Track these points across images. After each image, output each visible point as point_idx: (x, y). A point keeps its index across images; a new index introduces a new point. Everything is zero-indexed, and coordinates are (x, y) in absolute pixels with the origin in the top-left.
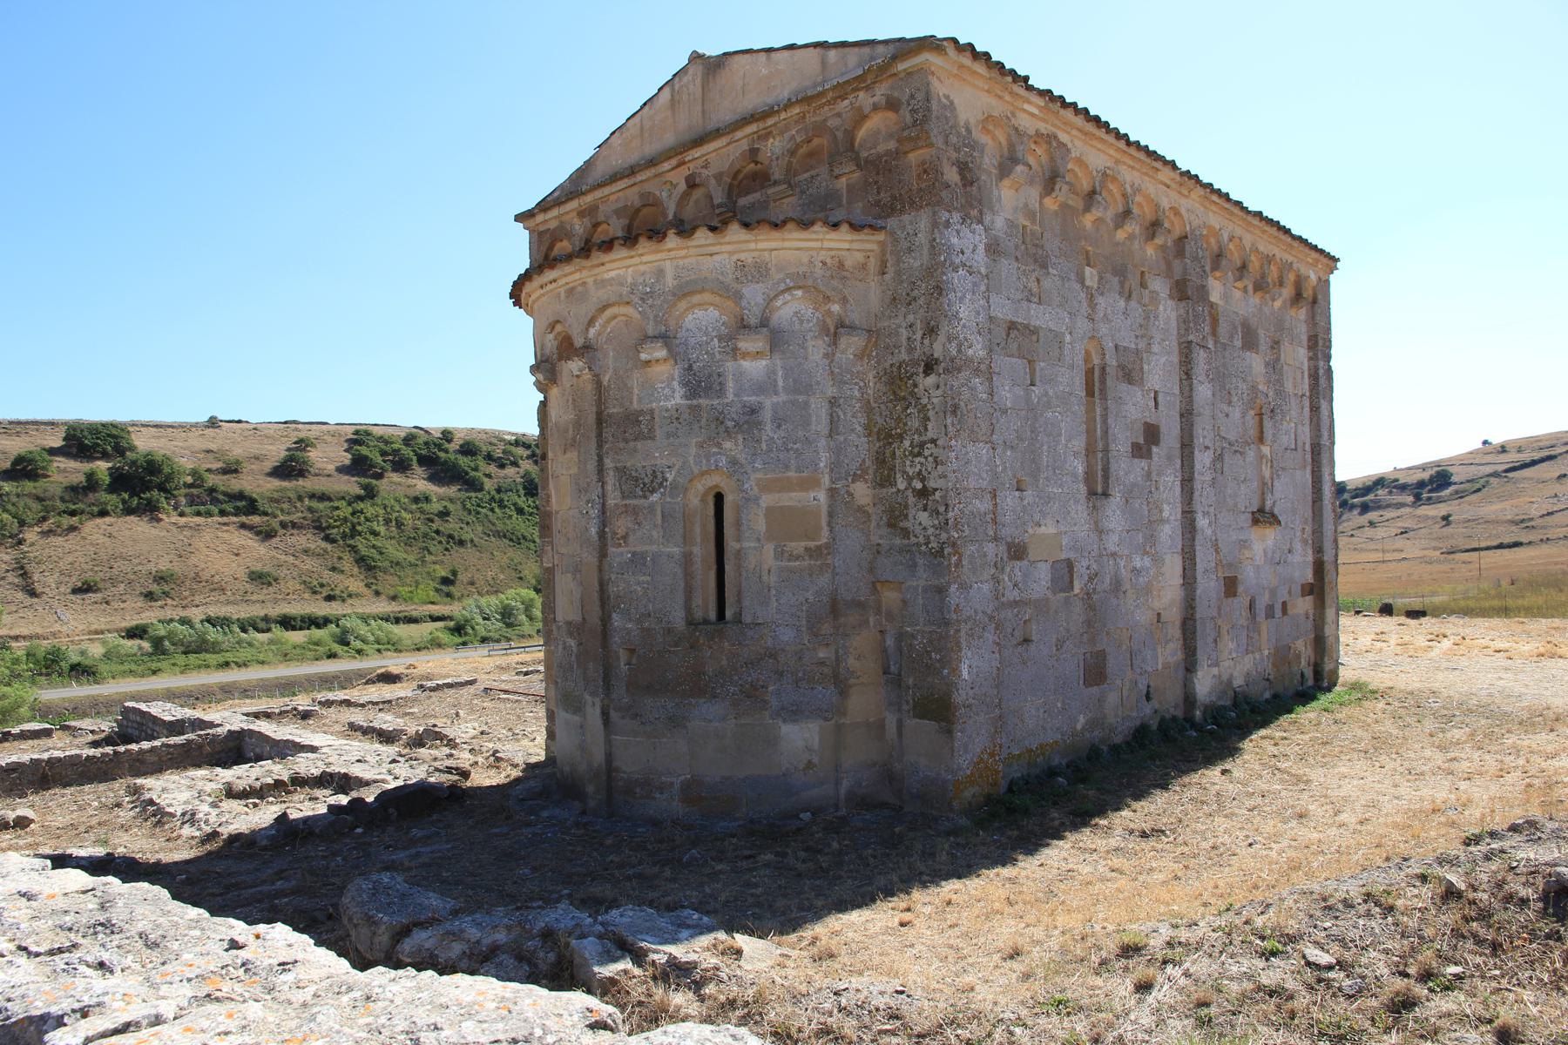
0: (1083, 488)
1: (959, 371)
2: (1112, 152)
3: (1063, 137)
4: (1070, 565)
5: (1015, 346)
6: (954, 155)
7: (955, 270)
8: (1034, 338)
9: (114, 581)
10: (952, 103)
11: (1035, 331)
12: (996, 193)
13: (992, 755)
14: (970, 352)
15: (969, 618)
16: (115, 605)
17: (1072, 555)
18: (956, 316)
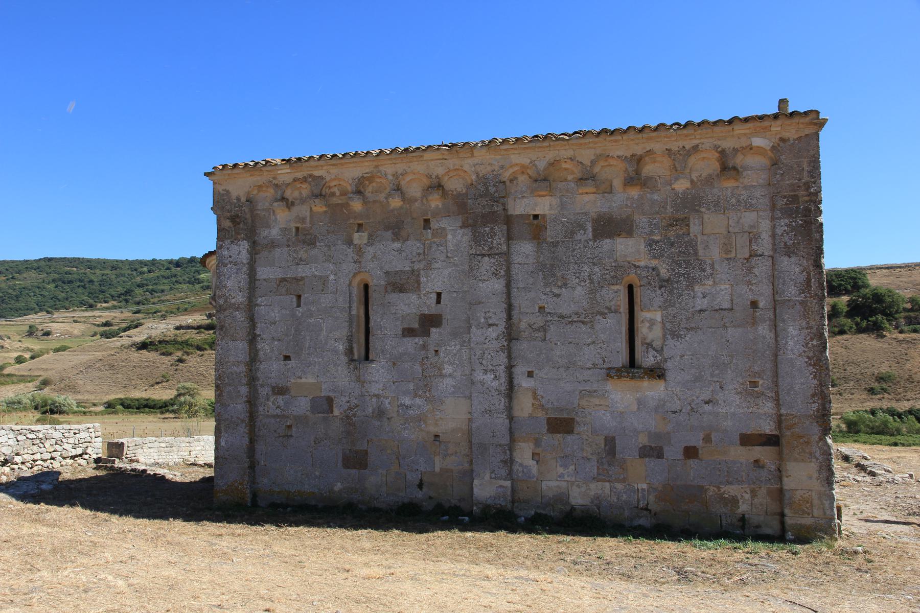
0: (344, 359)
1: (225, 310)
2: (367, 164)
3: (317, 173)
4: (330, 401)
5: (284, 290)
6: (229, 214)
7: (226, 265)
8: (301, 283)
9: (846, 379)
10: (228, 191)
11: (302, 279)
12: (273, 218)
13: (241, 484)
14: (233, 301)
15: (227, 419)
16: (846, 396)
17: (331, 394)
18: (225, 287)
